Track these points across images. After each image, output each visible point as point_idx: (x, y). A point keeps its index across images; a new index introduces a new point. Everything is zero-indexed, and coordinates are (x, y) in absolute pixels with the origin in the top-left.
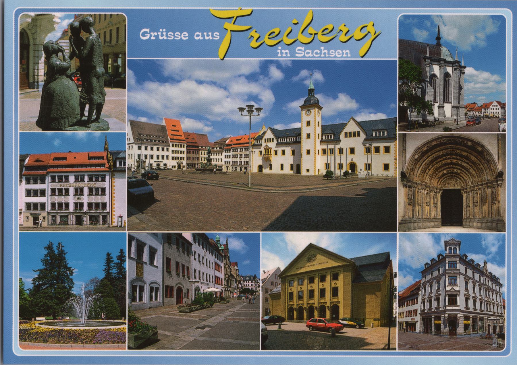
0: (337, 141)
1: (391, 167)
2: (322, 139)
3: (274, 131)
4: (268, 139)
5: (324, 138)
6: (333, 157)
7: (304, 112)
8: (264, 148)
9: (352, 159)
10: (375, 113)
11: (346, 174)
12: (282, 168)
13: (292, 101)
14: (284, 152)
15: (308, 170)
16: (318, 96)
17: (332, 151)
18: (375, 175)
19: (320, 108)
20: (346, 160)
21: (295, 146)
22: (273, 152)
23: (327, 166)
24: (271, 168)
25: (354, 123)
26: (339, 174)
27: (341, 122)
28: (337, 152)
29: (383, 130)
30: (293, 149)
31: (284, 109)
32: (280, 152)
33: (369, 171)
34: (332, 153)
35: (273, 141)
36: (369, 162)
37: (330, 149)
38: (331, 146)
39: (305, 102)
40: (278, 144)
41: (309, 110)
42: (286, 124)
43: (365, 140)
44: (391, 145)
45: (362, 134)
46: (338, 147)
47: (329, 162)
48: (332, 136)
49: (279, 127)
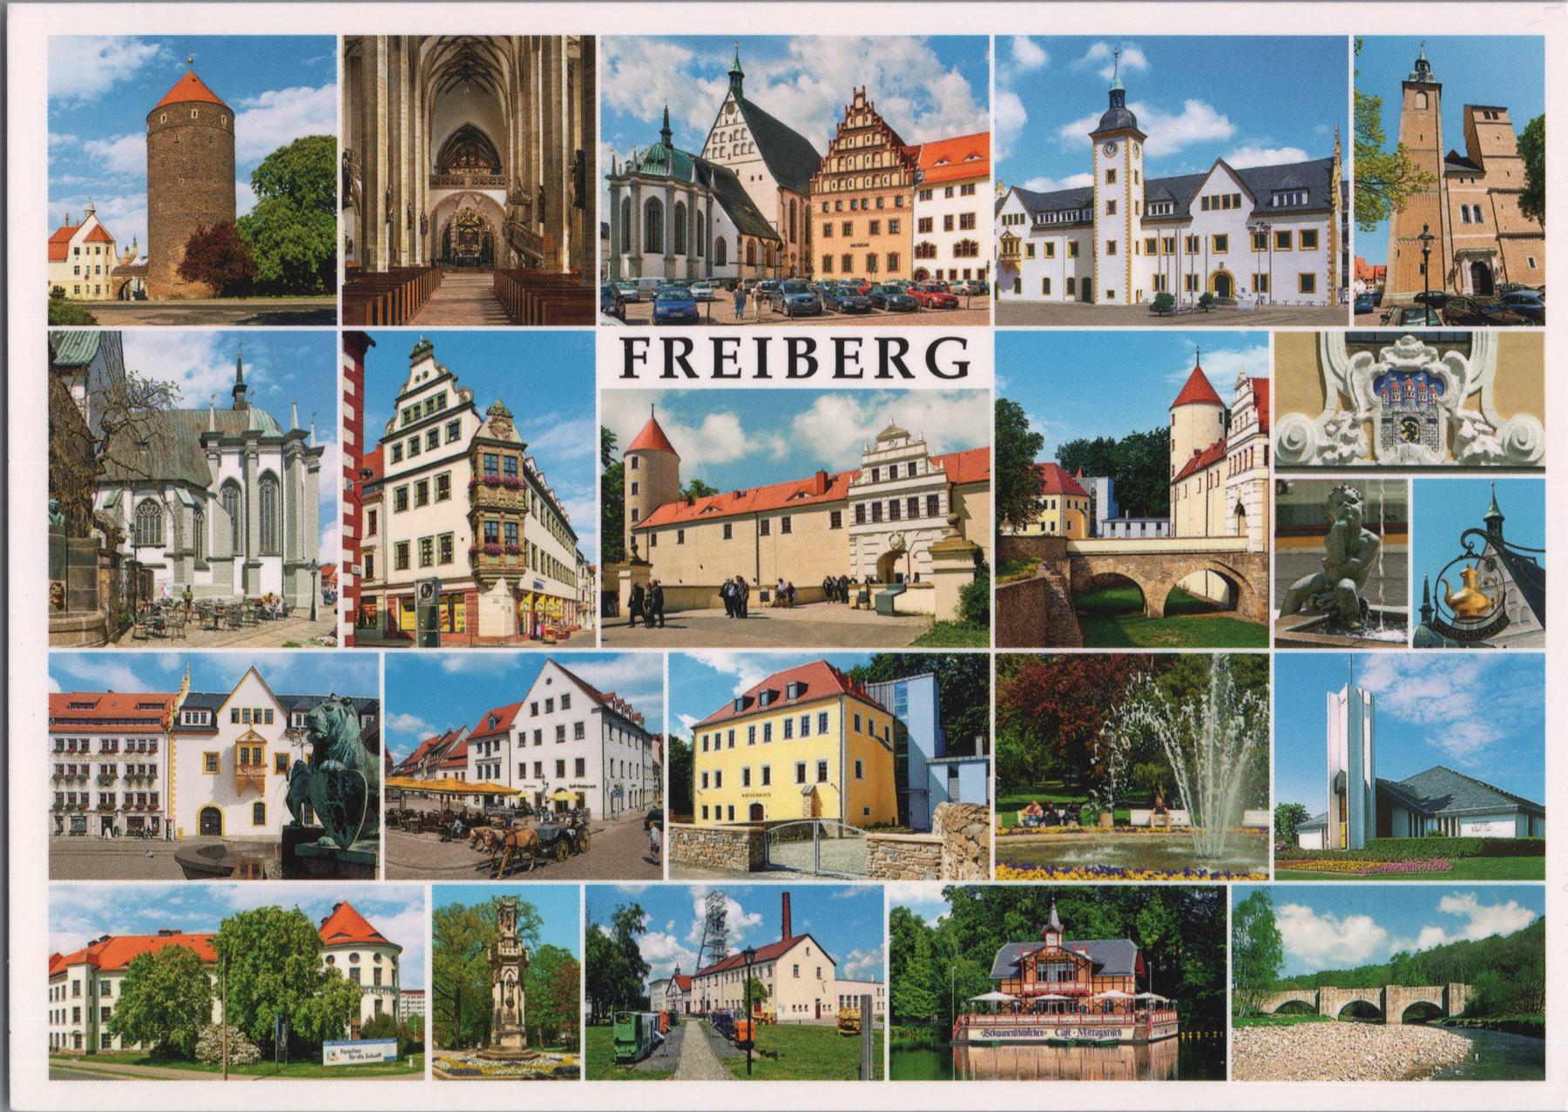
0: (1184, 218)
1: (1321, 284)
2: (1146, 213)
3: (1025, 196)
4: (1010, 216)
5: (1150, 213)
6: (1172, 258)
7: (1100, 147)
8: (1002, 240)
9: (1222, 264)
10: (1278, 148)
11: (1206, 301)
12: (1047, 289)
13: (1071, 119)
14: (1050, 249)
15: (1111, 294)
16: (1135, 108)
17: (1171, 245)
18: (1280, 302)
19: (1141, 138)
20: (1205, 265)
21: (1078, 235)
22: (1023, 250)
23: (1159, 281)
24: (1018, 290)
25: (1226, 175)
26: (1188, 301)
27: (1194, 171)
28: (1182, 245)
29: (1299, 190)
30: (1072, 240)
31: (1050, 139)
32: (1040, 249)
33: (1263, 294)
34: (1172, 250)
35: (1023, 222)
36: (1264, 270)
37: (1166, 240)
38: (1168, 232)
39: (1102, 122)
40: (1036, 229)
41: (1113, 145)
42: (1056, 179)
43: (1253, 215)
44: (1321, 226)
45: (1245, 200)
46: (1185, 232)
47: (1164, 271)
48: (1171, 207)
49: (1038, 186)
